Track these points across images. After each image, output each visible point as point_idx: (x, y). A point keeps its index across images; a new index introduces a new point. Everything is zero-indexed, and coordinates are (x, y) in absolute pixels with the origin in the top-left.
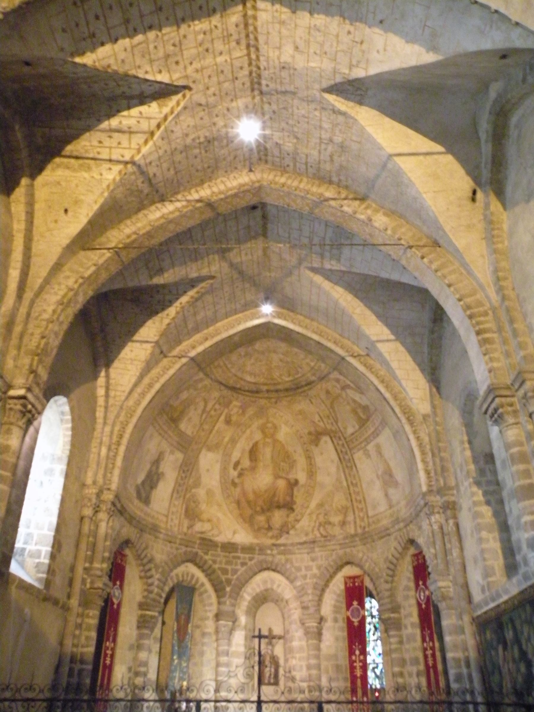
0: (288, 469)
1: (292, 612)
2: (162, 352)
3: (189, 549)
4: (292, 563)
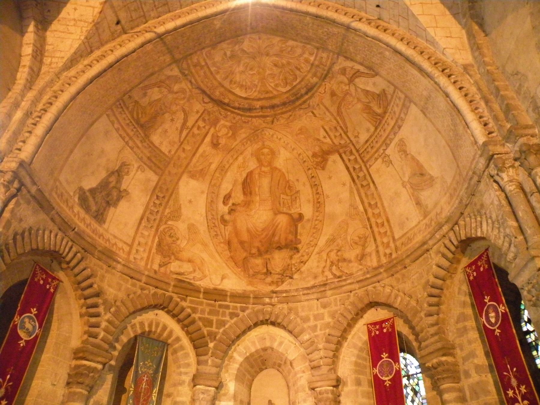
0: (290, 202)
1: (298, 376)
2: (118, 23)
3: (160, 292)
4: (297, 314)
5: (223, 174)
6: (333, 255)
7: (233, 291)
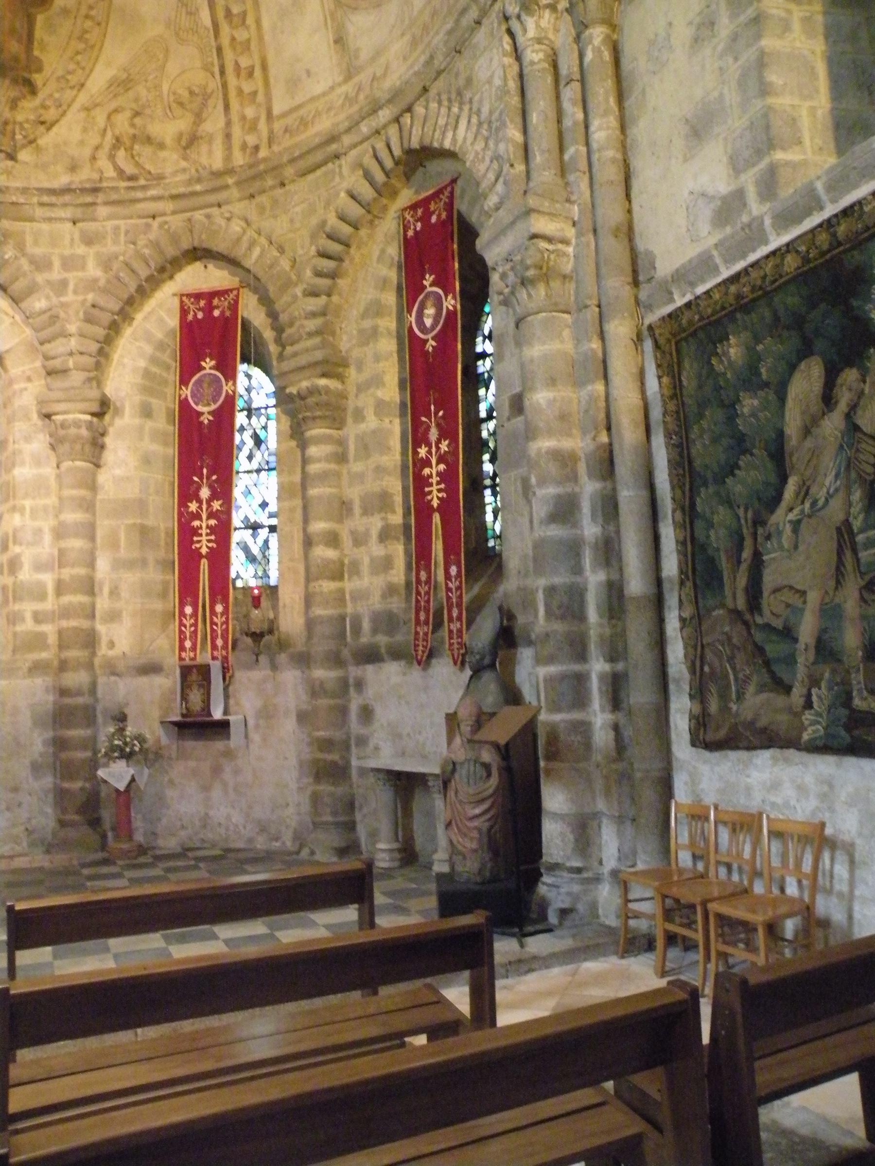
1: (16, 387)
4: (21, 247)
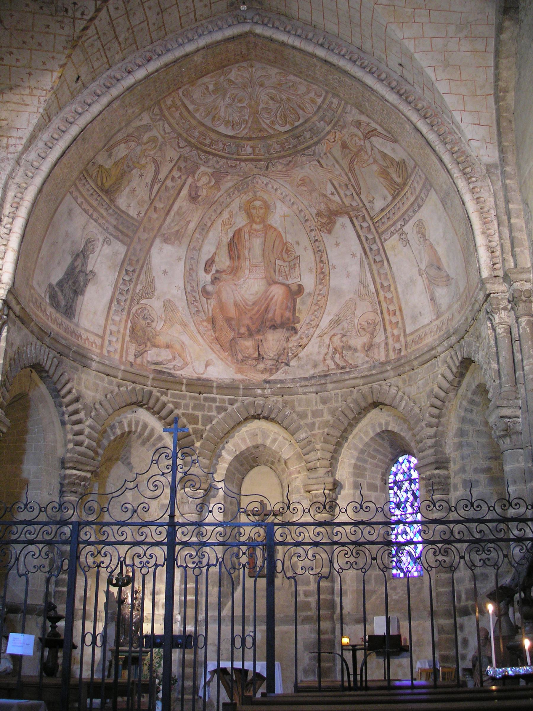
0: (287, 269)
1: (293, 476)
3: (139, 387)
4: (293, 408)
5: (204, 233)
6: (337, 340)
7: (219, 381)
